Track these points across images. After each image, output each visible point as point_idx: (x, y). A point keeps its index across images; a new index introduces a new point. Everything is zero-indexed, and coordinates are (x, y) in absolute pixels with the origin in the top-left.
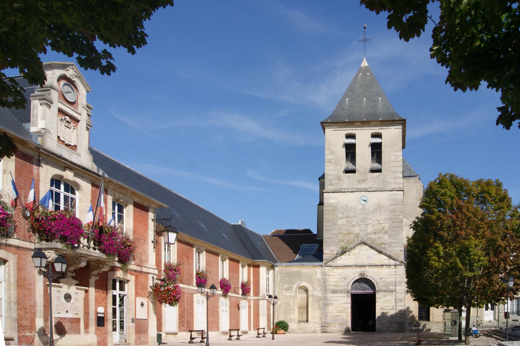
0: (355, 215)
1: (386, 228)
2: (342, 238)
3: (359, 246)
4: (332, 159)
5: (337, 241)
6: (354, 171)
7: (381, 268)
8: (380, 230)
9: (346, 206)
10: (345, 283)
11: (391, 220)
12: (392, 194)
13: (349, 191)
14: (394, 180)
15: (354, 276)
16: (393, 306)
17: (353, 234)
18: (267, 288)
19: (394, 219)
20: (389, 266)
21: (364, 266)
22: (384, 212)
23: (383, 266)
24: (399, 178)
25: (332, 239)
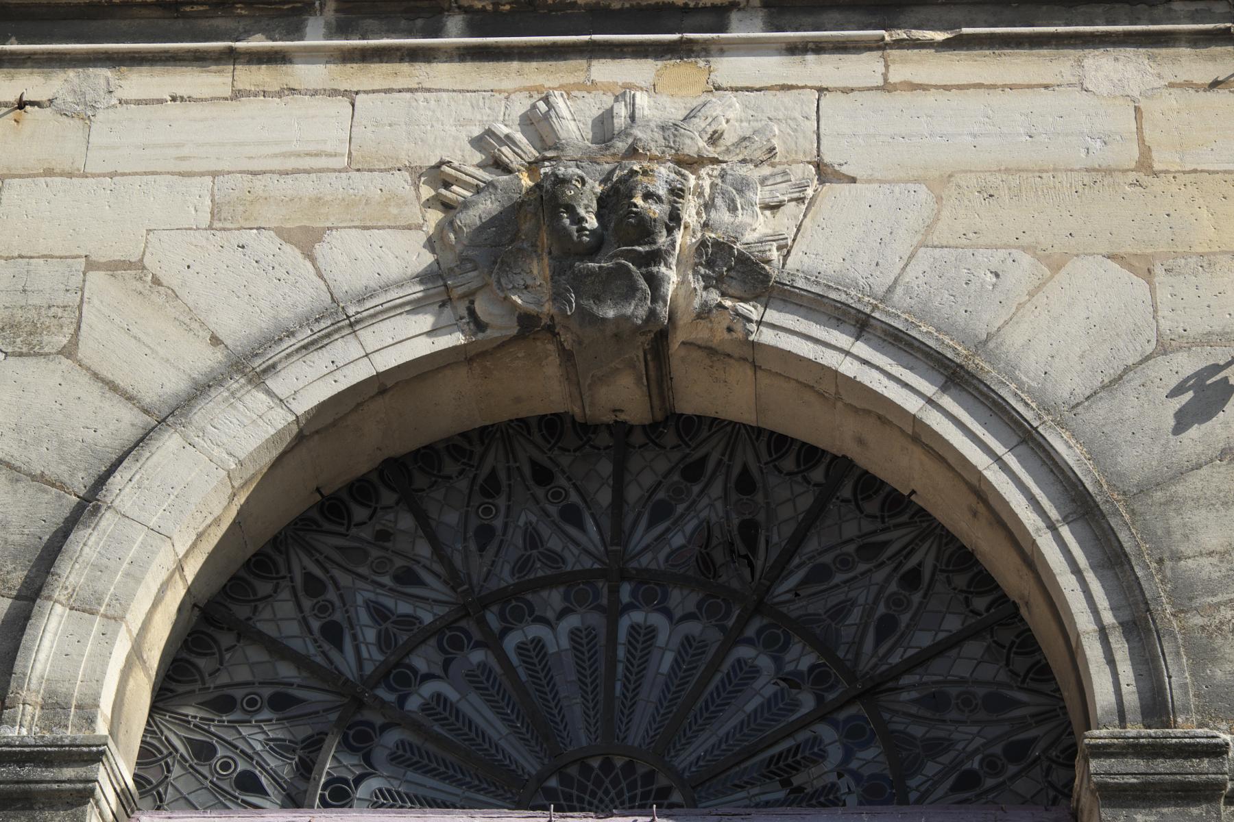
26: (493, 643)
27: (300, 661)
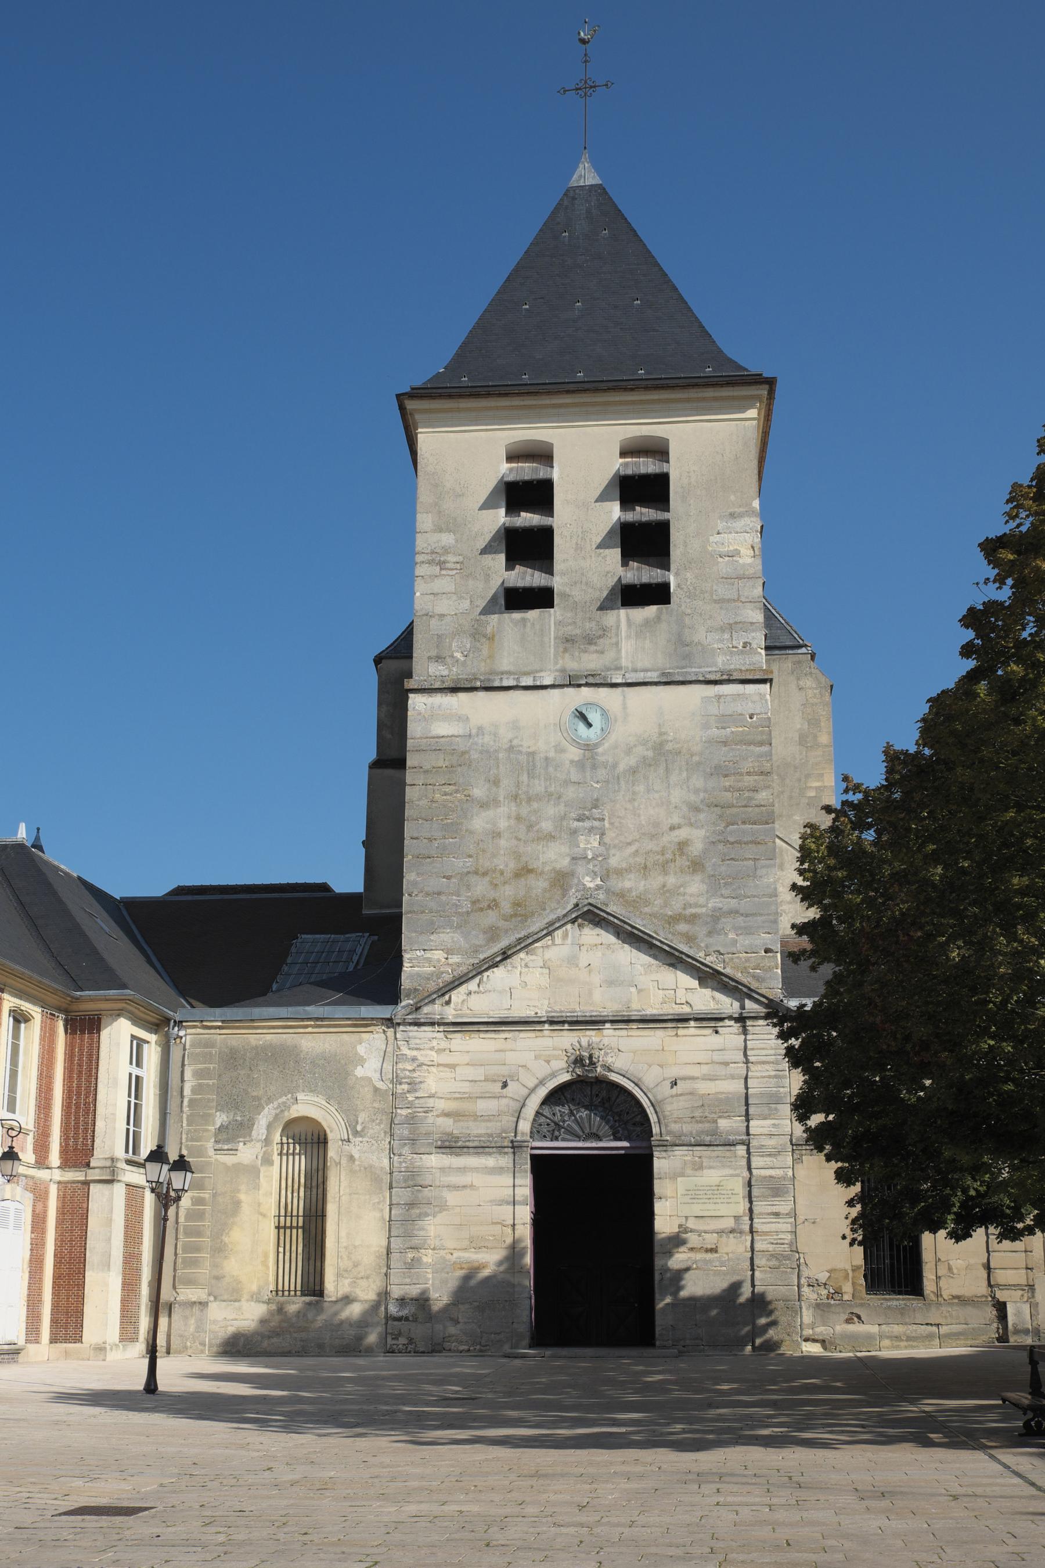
0: (552, 789)
1: (697, 848)
2: (492, 894)
3: (569, 926)
4: (446, 551)
5: (466, 906)
6: (542, 598)
7: (672, 1032)
8: (669, 856)
9: (511, 749)
10: (504, 1101)
11: (718, 810)
12: (719, 697)
13: (523, 684)
14: (726, 636)
15: (549, 1071)
16: (737, 1218)
17: (542, 873)
18: (132, 1128)
19: (733, 806)
20: (711, 1020)
21: (595, 1022)
22: (685, 774)
23: (682, 1020)
24: (748, 626)
25: (443, 898)
26: (574, 1116)
27: (550, 1119)
